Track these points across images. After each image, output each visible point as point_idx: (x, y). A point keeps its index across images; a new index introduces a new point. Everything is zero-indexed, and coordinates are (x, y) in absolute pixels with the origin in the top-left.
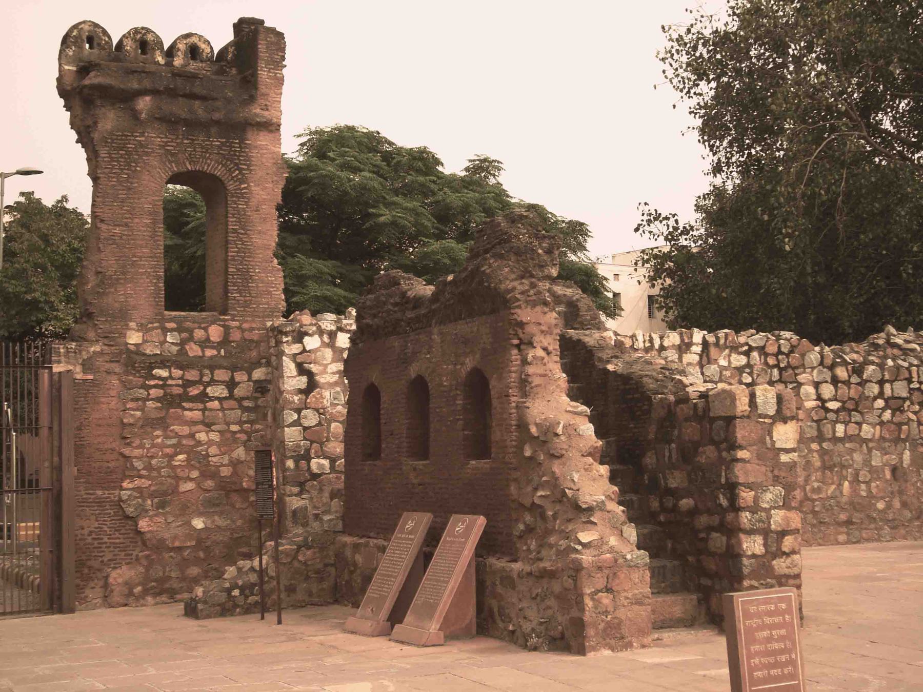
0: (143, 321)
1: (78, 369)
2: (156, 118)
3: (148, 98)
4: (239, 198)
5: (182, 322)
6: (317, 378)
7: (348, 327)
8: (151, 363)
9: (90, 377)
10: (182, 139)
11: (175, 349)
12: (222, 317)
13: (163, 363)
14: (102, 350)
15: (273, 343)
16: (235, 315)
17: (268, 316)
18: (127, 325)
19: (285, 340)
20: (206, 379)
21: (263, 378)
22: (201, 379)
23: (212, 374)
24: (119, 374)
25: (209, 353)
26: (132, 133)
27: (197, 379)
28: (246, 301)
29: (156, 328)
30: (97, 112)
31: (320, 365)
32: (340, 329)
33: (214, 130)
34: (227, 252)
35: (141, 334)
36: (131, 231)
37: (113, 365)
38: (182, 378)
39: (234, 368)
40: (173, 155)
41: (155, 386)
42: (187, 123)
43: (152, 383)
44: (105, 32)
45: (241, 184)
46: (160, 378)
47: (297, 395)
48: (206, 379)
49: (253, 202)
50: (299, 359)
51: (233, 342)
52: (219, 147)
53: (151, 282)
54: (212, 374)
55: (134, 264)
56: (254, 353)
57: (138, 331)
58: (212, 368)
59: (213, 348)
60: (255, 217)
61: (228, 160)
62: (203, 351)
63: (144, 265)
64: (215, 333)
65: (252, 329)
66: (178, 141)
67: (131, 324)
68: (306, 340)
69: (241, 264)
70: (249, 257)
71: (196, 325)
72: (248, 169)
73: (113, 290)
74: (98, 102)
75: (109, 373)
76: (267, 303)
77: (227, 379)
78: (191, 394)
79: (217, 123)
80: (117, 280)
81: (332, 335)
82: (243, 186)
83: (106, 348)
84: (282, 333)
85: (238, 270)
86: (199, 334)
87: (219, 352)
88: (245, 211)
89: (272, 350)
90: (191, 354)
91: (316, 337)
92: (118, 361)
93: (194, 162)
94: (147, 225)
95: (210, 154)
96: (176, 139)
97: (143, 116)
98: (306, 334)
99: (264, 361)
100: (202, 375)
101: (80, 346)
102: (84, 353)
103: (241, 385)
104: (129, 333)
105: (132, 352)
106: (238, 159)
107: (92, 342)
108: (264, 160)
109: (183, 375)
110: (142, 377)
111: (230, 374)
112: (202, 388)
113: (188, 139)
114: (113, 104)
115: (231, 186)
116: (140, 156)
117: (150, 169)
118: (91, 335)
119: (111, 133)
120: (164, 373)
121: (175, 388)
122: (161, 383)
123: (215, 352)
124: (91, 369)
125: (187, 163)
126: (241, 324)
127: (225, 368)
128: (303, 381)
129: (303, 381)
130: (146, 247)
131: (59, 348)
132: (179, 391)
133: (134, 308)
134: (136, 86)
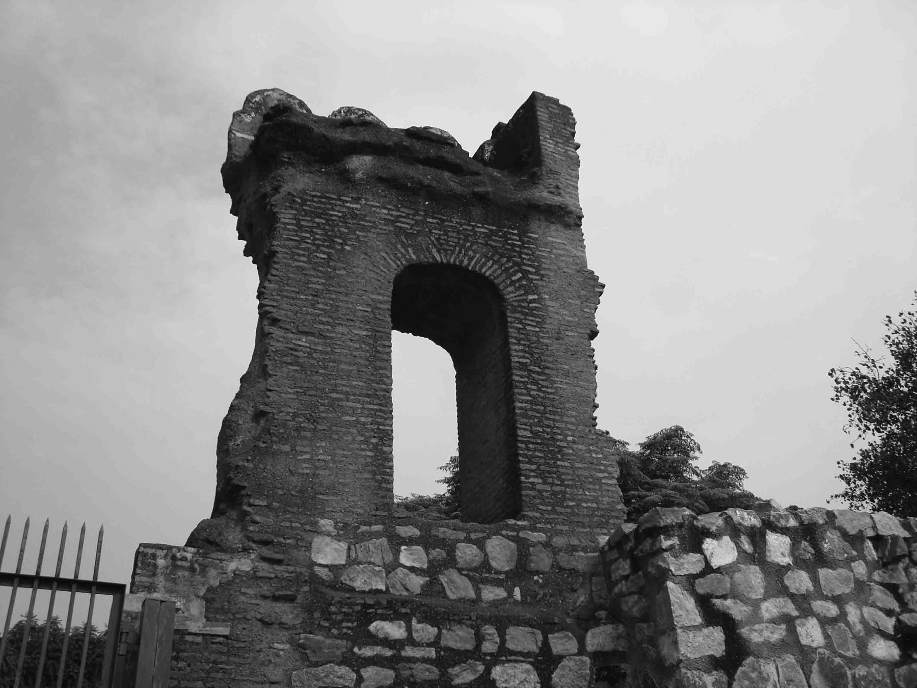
0: (349, 519)
1: (196, 608)
2: (381, 180)
3: (367, 158)
4: (526, 314)
6: (744, 631)
7: (783, 523)
8: (365, 606)
9: (224, 630)
10: (426, 216)
11: (417, 582)
12: (511, 522)
13: (395, 608)
14: (255, 570)
15: (624, 567)
16: (536, 520)
17: (600, 525)
18: (317, 522)
19: (666, 544)
20: (489, 647)
21: (609, 647)
22: (478, 647)
23: (502, 635)
24: (294, 627)
25: (491, 593)
27: (470, 646)
28: (554, 494)
29: (378, 535)
30: (279, 172)
31: (746, 601)
33: (477, 212)
34: (509, 400)
35: (344, 545)
36: (325, 344)
37: (280, 607)
38: (435, 643)
39: (547, 627)
42: (432, 194)
44: (302, 104)
45: (527, 293)
46: (387, 642)
47: (708, 672)
48: (489, 647)
49: (551, 325)
50: (702, 586)
51: (537, 573)
52: (487, 236)
53: (366, 442)
54: (502, 635)
55: (333, 405)
56: (582, 598)
59: (498, 583)
60: (554, 346)
61: (502, 256)
62: (478, 592)
64: (500, 551)
65: (572, 549)
68: (709, 545)
70: (555, 413)
71: (462, 535)
72: (537, 273)
73: (287, 448)
75: (266, 624)
76: (596, 500)
77: (534, 649)
78: (457, 681)
79: (482, 198)
80: (298, 429)
81: (757, 537)
82: (531, 297)
83: (265, 565)
84: (655, 532)
85: (536, 434)
86: (467, 553)
87: (510, 594)
88: (538, 336)
90: (452, 596)
91: (726, 539)
92: (291, 599)
93: (446, 250)
94: (361, 340)
95: (472, 243)
96: (414, 215)
97: (359, 175)
98: (706, 533)
99: (602, 614)
100: (479, 638)
101: (205, 556)
102: (212, 573)
103: (565, 662)
104: (317, 541)
105: (322, 582)
106: (520, 257)
108: (563, 265)
109: (439, 636)
110: (341, 636)
111: (540, 637)
112: (481, 668)
113: (433, 218)
114: (308, 163)
115: (511, 295)
118: (234, 536)
119: (304, 192)
120: (394, 630)
121: (420, 666)
122: (388, 653)
123: (501, 593)
124: (222, 610)
125: (434, 251)
126: (550, 538)
127: (529, 623)
128: (713, 641)
129: (713, 641)
130: (359, 377)
131: (154, 556)
132: (433, 673)
133: (332, 489)
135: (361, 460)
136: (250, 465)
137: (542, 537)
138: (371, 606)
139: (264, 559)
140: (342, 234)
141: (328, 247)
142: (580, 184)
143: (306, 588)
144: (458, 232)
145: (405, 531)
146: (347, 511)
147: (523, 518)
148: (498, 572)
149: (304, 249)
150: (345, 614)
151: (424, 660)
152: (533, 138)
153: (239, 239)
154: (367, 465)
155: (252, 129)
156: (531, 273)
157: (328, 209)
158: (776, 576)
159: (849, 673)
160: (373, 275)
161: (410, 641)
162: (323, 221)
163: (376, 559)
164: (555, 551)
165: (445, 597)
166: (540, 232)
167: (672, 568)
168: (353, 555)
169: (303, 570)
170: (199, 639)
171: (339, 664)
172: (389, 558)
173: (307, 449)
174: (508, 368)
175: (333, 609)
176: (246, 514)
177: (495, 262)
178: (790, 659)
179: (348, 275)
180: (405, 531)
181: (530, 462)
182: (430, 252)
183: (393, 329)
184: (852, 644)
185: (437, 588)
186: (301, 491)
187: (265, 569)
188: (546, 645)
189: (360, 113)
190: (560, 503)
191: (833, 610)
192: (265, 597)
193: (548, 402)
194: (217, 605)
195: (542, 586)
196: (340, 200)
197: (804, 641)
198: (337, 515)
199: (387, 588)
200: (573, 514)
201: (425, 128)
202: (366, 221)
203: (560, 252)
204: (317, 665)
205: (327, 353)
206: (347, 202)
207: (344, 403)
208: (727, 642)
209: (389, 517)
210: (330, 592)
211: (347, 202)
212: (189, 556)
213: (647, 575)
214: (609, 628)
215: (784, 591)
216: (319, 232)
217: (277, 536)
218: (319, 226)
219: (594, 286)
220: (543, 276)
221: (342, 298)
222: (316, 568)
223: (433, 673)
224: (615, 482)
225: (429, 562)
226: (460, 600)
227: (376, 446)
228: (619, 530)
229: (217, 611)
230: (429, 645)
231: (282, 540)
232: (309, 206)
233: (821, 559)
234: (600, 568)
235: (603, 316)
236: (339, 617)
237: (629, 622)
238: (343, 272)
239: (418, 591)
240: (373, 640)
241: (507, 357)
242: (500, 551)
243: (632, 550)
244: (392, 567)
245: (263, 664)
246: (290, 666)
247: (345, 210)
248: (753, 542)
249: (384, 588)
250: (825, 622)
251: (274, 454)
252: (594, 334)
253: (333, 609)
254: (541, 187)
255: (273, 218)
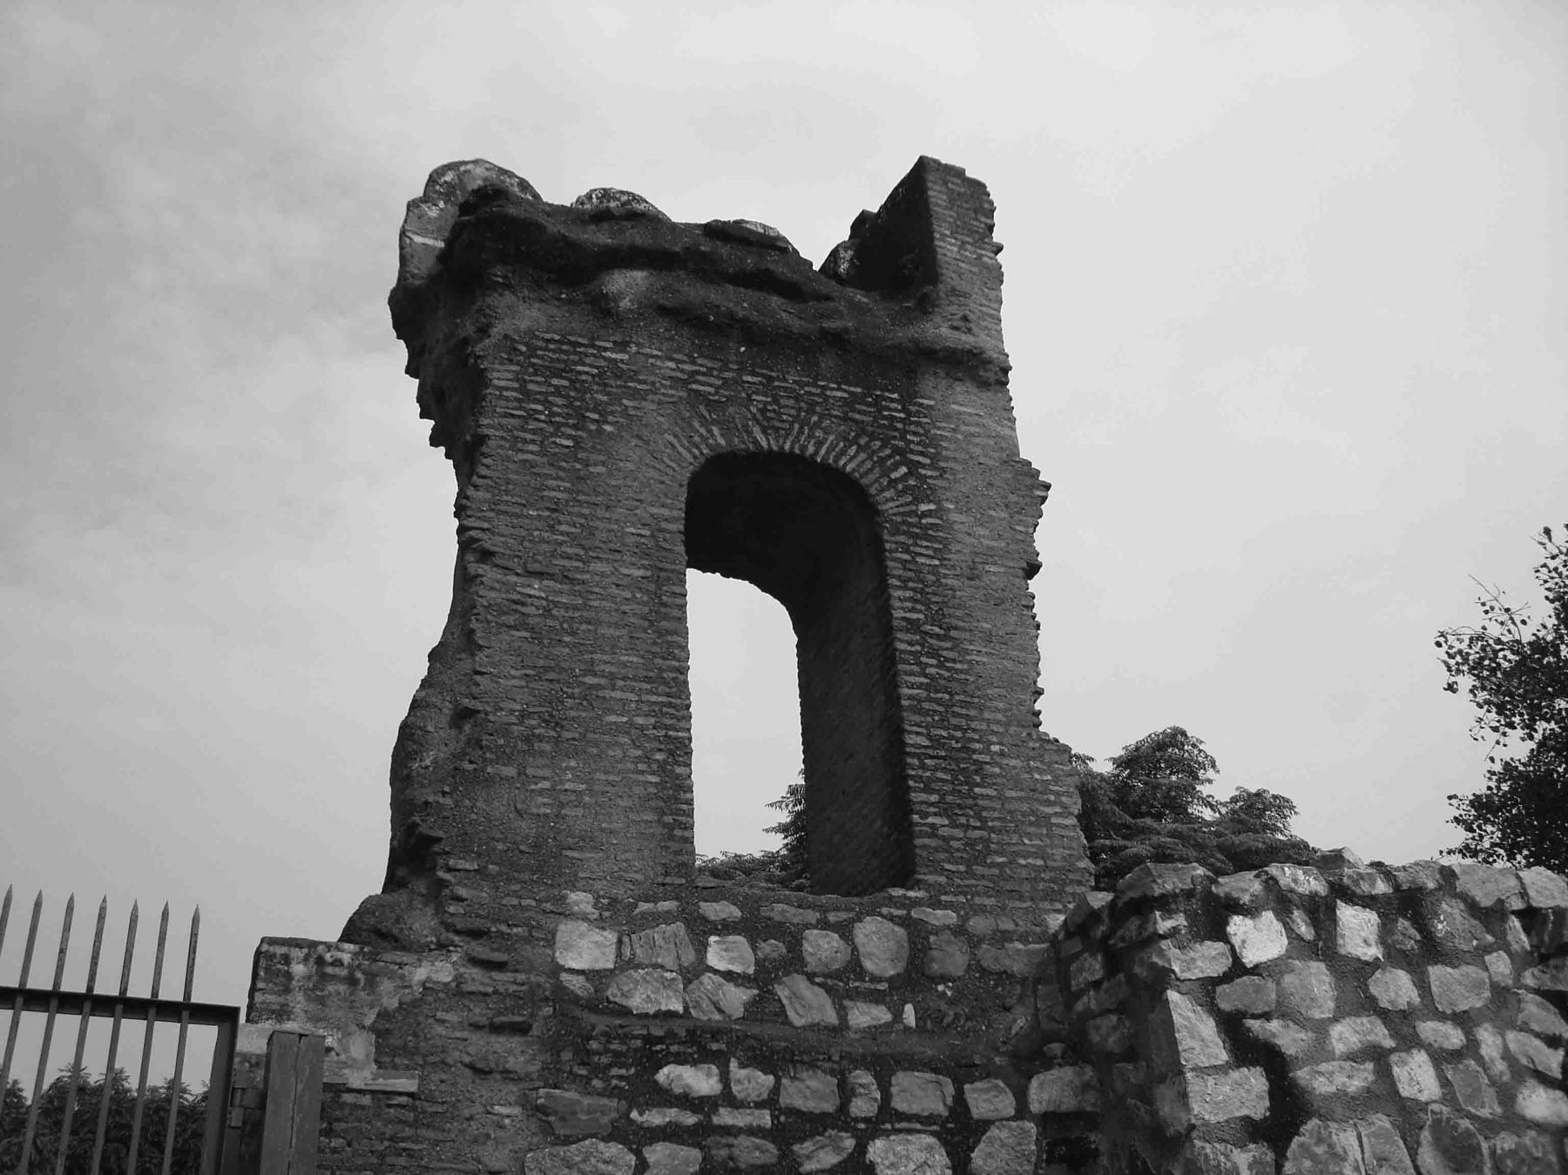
0: (619, 892)
1: (360, 1046)
2: (663, 311)
3: (639, 276)
5: (758, 901)
6: (1302, 1075)
7: (1365, 887)
8: (649, 1040)
9: (410, 1085)
10: (742, 370)
11: (736, 998)
12: (897, 892)
13: (699, 1042)
14: (459, 980)
15: (1093, 967)
17: (1049, 896)
18: (565, 897)
19: (1164, 925)
20: (862, 1107)
21: (1069, 1104)
22: (843, 1107)
24: (528, 1075)
25: (865, 1016)
26: (593, 339)
27: (829, 1107)
28: (971, 843)
29: (667, 918)
30: (489, 300)
31: (1303, 1022)
32: (1342, 892)
33: (827, 362)
35: (611, 936)
36: (574, 593)
37: (501, 1043)
38: (770, 1102)
39: (962, 1071)
40: (711, 405)
41: (670, 1133)
42: (749, 333)
43: (655, 1118)
44: (524, 185)
45: (917, 500)
46: (687, 1101)
47: (1242, 1146)
48: (862, 1107)
49: (960, 554)
50: (1228, 998)
51: (944, 979)
52: (850, 403)
53: (647, 759)
55: (589, 697)
57: (601, 924)
58: (884, 1068)
59: (876, 998)
60: (965, 591)
61: (872, 437)
62: (842, 1012)
63: (624, 702)
65: (1001, 938)
66: (727, 375)
67: (574, 897)
68: (1238, 926)
69: (943, 723)
71: (812, 916)
72: (933, 467)
73: (510, 771)
74: (498, 273)
75: (480, 1072)
78: (809, 1166)
79: (837, 340)
80: (527, 740)
81: (1321, 912)
82: (924, 507)
83: (476, 972)
84: (1145, 906)
85: (937, 742)
86: (822, 947)
87: (898, 1015)
89: (1089, 1001)
90: (798, 1022)
91: (1268, 916)
92: (521, 1029)
93: (777, 429)
94: (635, 584)
95: (821, 417)
96: (721, 370)
97: (625, 304)
98: (1233, 907)
99: (1056, 1048)
100: (846, 1093)
102: (386, 986)
103: (994, 1132)
104: (565, 929)
105: (576, 1000)
106: (903, 438)
107: (420, 950)
108: (977, 451)
109: (776, 1090)
111: (950, 1089)
112: (849, 1143)
113: (754, 374)
114: (538, 285)
115: (890, 503)
116: (616, 399)
117: (645, 432)
118: (422, 924)
119: (531, 333)
120: (700, 1080)
121: (744, 1141)
122: (690, 1119)
123: (882, 1015)
124: (405, 1050)
126: (965, 919)
128: (1247, 1092)
129: (1247, 1092)
130: (632, 649)
131: (286, 959)
132: (766, 1153)
133: (587, 840)
134: (602, 237)
135: (638, 790)
136: (448, 801)
137: (951, 917)
138: (660, 1040)
139: (474, 961)
140: (598, 404)
141: (575, 427)
142: (1003, 313)
143: (548, 1010)
144: (797, 398)
145: (717, 910)
146: (616, 879)
147: (917, 884)
148: (875, 979)
149: (534, 432)
150: (617, 1054)
151: (752, 1131)
152: (922, 236)
153: (422, 416)
154: (649, 798)
155: (440, 229)
156: (923, 466)
157: (576, 363)
158: (1354, 978)
159: (1485, 1146)
160: (653, 473)
161: (728, 1098)
162: (566, 383)
163: (667, 959)
164: (974, 942)
165: (787, 1022)
166: (938, 395)
167: (1176, 969)
168: (627, 952)
169: (542, 979)
170: (366, 1100)
171: (606, 1139)
172: (689, 957)
173: (547, 773)
174: (888, 631)
175: (594, 1045)
176: (442, 884)
177: (860, 448)
178: (1382, 1121)
179: (610, 474)
180: (717, 910)
181: (927, 789)
182: (750, 433)
183: (689, 566)
184: (1489, 1095)
185: (772, 1008)
186: (535, 846)
187: (476, 978)
188: (960, 1105)
189: (624, 198)
190: (981, 858)
191: (1454, 1037)
192: (477, 1027)
193: (955, 686)
194: (395, 1041)
195: (950, 1002)
196: (593, 346)
197: (1405, 1091)
198: (598, 885)
199: (686, 1009)
200: (1002, 876)
201: (736, 222)
202: (640, 382)
203: (973, 429)
204: (568, 1141)
205: (575, 608)
206: (605, 349)
207: (607, 693)
208: (1272, 1094)
209: (691, 888)
210: (593, 1018)
211: (605, 349)
212: (346, 958)
213: (1131, 978)
214: (1068, 1073)
215: (1370, 1006)
216: (559, 401)
217: (494, 921)
218: (558, 391)
219: (1031, 487)
220: (944, 470)
221: (601, 513)
222: (564, 976)
223: (766, 1153)
224: (1072, 821)
225: (757, 963)
226: (812, 1027)
227: (662, 765)
228: (1082, 901)
229: (394, 1052)
230: (760, 1105)
231: (504, 928)
232: (541, 358)
233: (1432, 950)
234: (1052, 970)
235: (1046, 539)
236: (605, 1060)
237: (1104, 1061)
238: (601, 469)
239: (739, 1012)
240: (665, 1097)
241: (885, 610)
242: (878, 943)
243: (1106, 937)
244: (693, 972)
245: (475, 1141)
246: (522, 1143)
247: (603, 364)
248: (1315, 922)
249: (680, 1008)
250: (1441, 1058)
251: (489, 782)
252: (1033, 569)
253: (594, 1045)
254: (938, 319)
255: (478, 380)
